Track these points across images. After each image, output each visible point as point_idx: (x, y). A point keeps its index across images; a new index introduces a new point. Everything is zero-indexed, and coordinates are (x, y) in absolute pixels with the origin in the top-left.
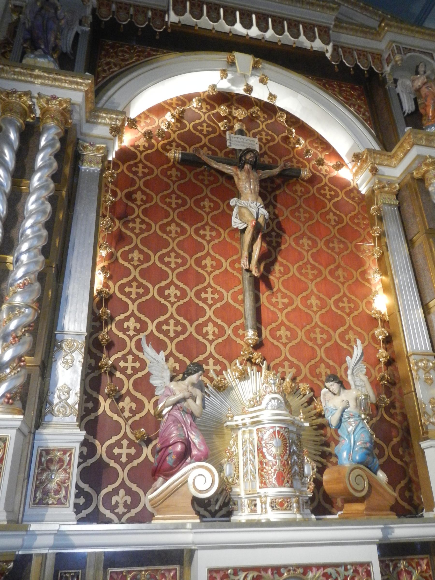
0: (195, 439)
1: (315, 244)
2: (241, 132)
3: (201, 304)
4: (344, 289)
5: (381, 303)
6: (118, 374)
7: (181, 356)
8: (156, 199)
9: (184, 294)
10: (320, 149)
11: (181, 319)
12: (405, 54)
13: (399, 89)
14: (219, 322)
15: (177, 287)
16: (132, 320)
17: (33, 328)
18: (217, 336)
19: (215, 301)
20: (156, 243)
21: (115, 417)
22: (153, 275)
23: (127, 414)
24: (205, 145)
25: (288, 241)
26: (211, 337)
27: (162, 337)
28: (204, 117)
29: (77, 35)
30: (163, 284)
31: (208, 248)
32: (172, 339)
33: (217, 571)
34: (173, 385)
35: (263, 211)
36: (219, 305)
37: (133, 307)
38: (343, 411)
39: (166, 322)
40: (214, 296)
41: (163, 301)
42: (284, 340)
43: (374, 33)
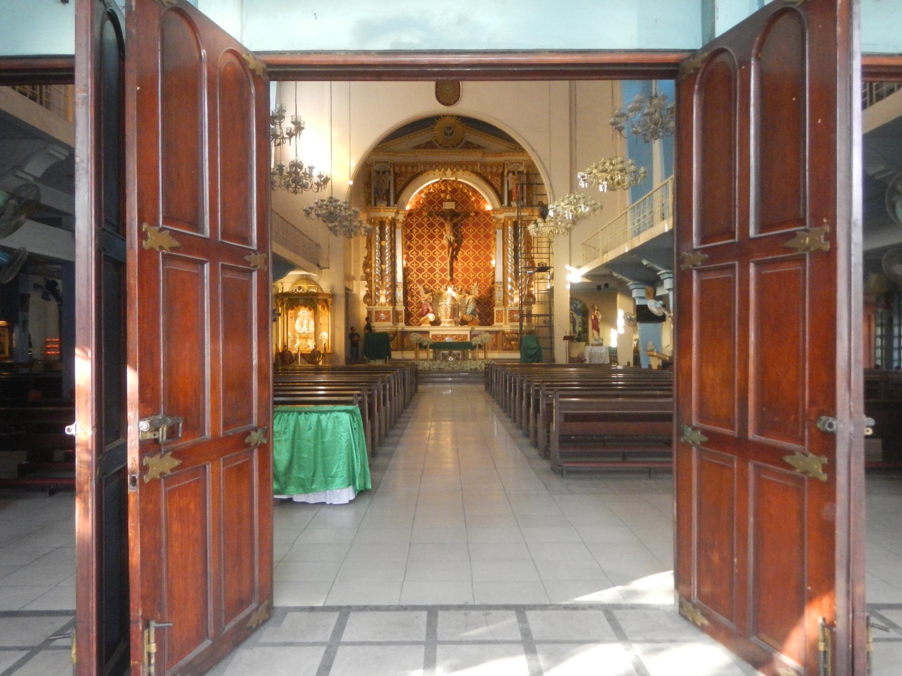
0: (430, 309)
2: (449, 200)
4: (482, 259)
5: (493, 262)
8: (420, 231)
17: (391, 286)
20: (420, 248)
22: (420, 259)
25: (465, 242)
31: (437, 248)
35: (452, 238)
40: (438, 266)
43: (499, 153)
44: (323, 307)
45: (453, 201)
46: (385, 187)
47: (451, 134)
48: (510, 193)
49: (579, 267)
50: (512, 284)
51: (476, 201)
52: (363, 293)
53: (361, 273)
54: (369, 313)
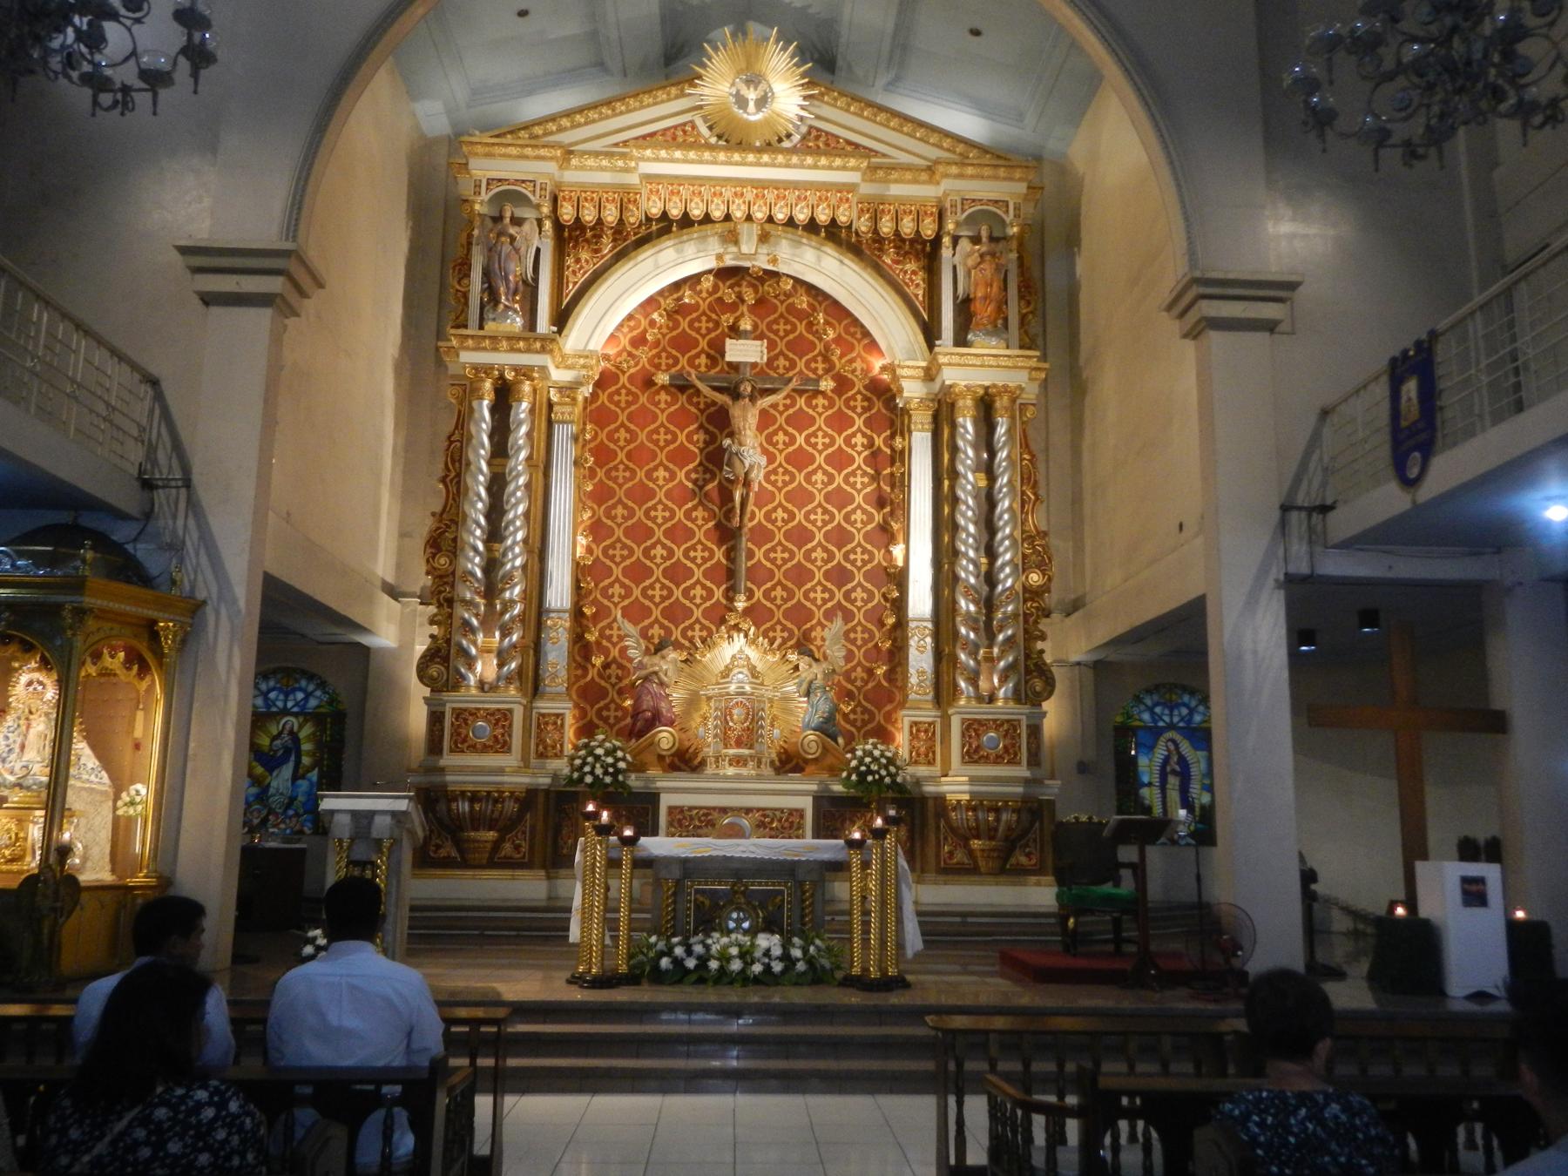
1: (831, 478)
3: (689, 564)
6: (605, 643)
7: (666, 623)
9: (671, 553)
10: (859, 336)
11: (667, 582)
12: (963, 211)
13: (957, 259)
14: (708, 584)
15: (664, 546)
16: (617, 586)
18: (704, 599)
19: (705, 560)
21: (603, 683)
23: (613, 680)
24: (703, 351)
26: (698, 601)
27: (647, 603)
28: (704, 306)
29: (538, 250)
30: (649, 543)
32: (657, 605)
33: (676, 808)
34: (646, 660)
36: (708, 564)
37: (617, 572)
38: (811, 682)
39: (652, 587)
41: (648, 563)
42: (779, 602)
44: (137, 661)
45: (760, 337)
46: (517, 270)
47: (762, 102)
48: (964, 308)
49: (1325, 509)
50: (972, 622)
51: (838, 340)
52: (420, 648)
53: (422, 580)
54: (435, 719)
